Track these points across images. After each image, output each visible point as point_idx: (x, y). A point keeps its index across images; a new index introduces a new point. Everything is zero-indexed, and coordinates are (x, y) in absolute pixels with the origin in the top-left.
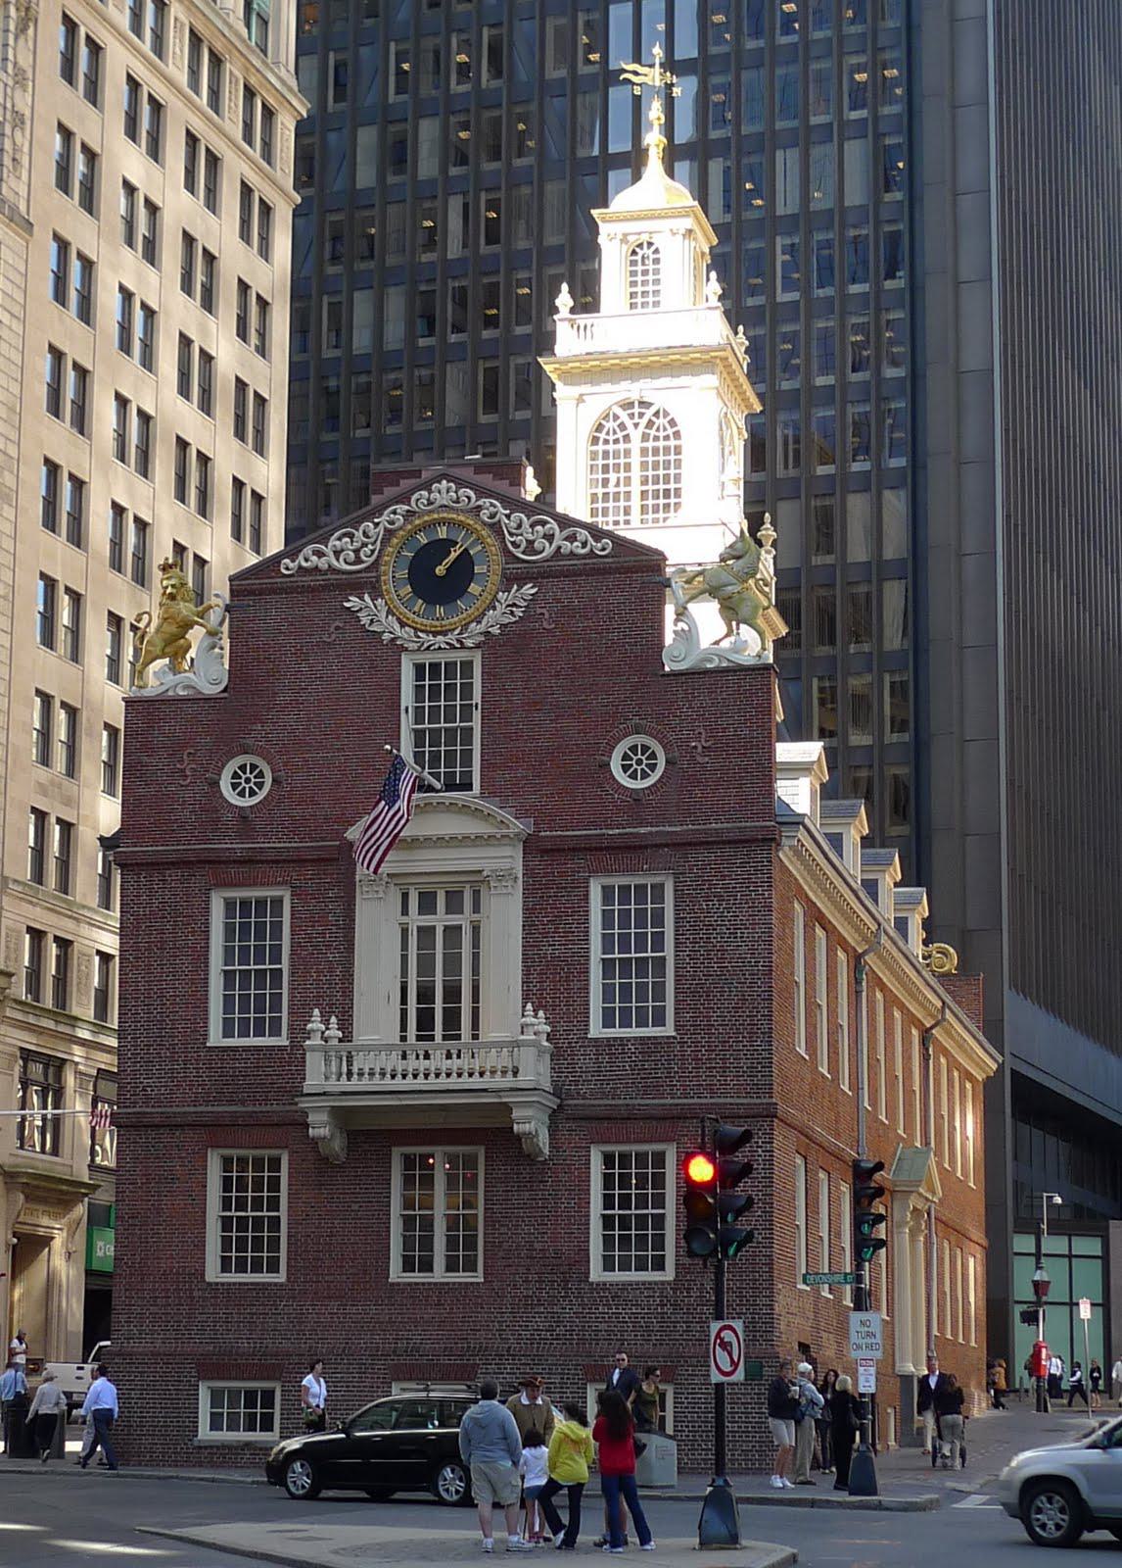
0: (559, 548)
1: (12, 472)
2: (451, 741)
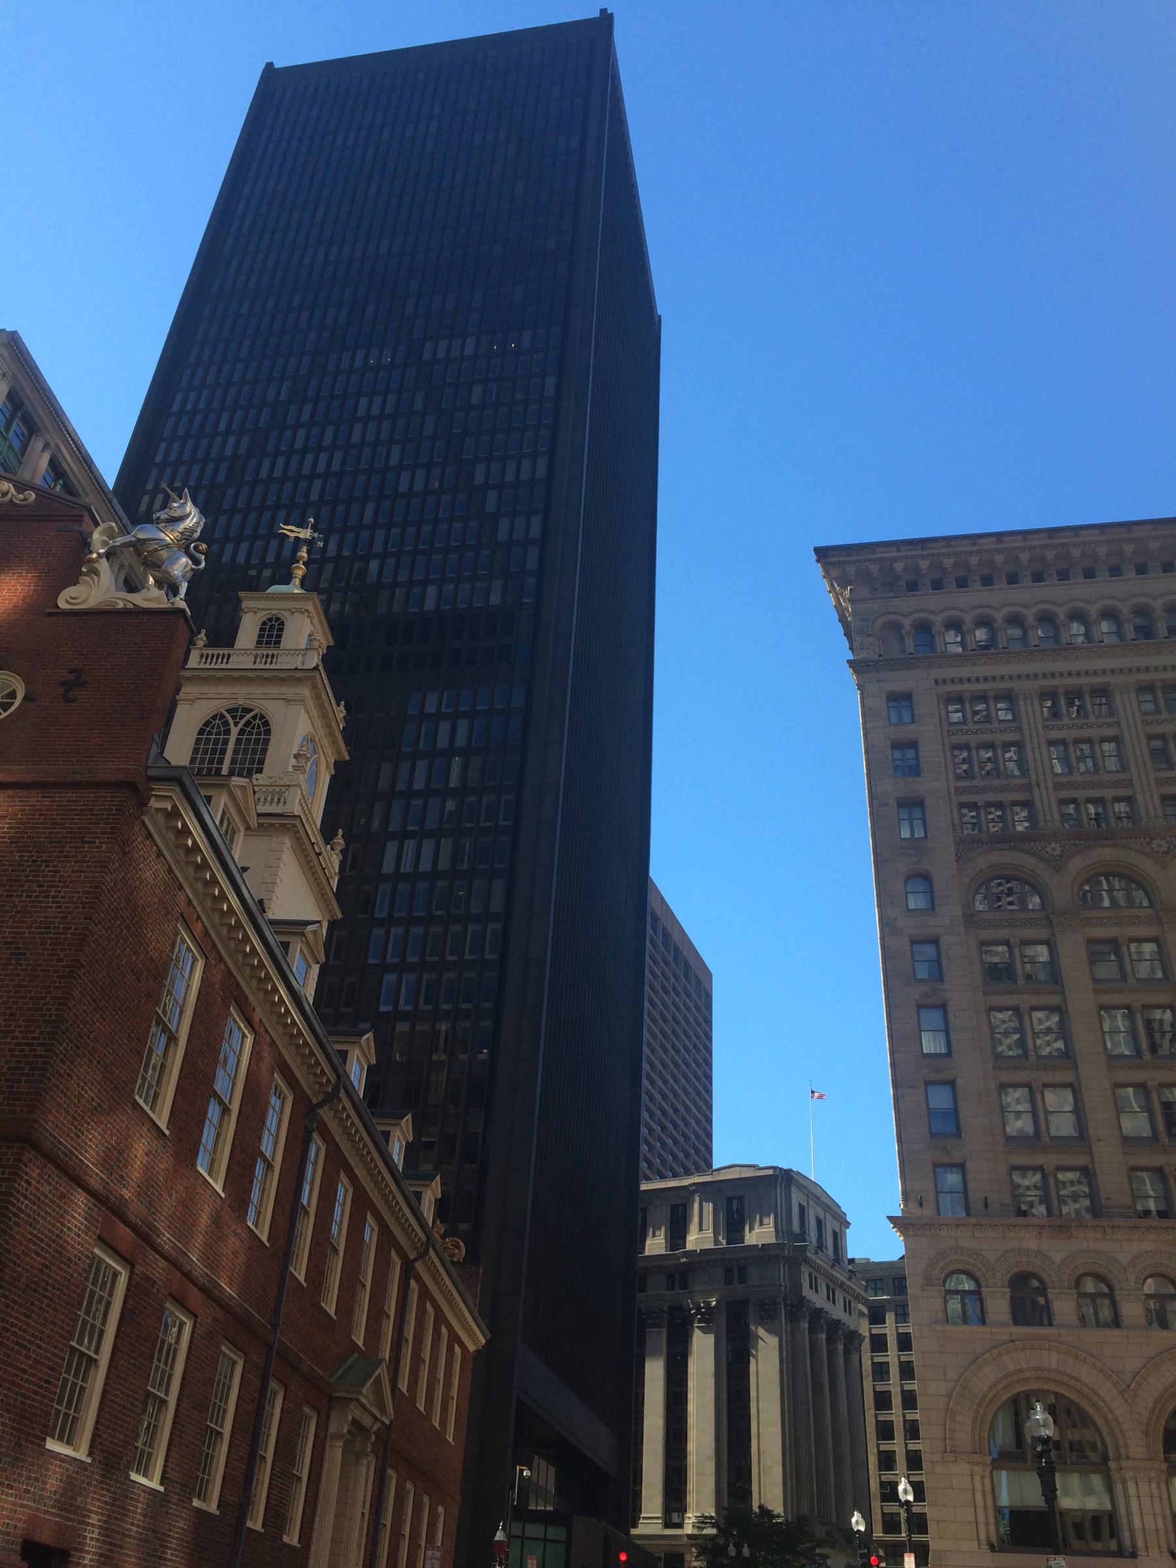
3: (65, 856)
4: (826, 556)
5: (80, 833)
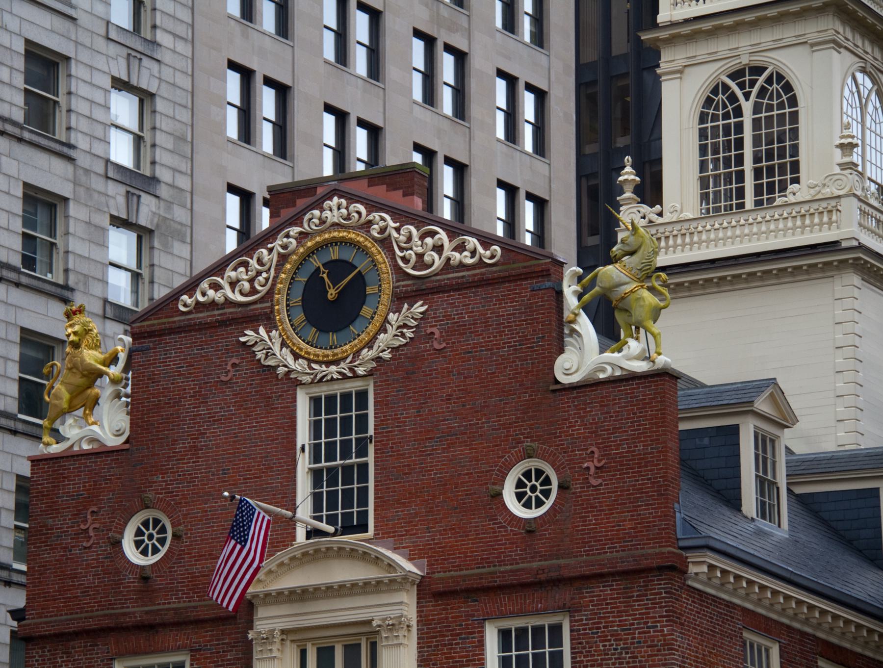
0: (449, 259)
1: (184, 206)
2: (347, 480)
3: (638, 642)
5: (642, 618)
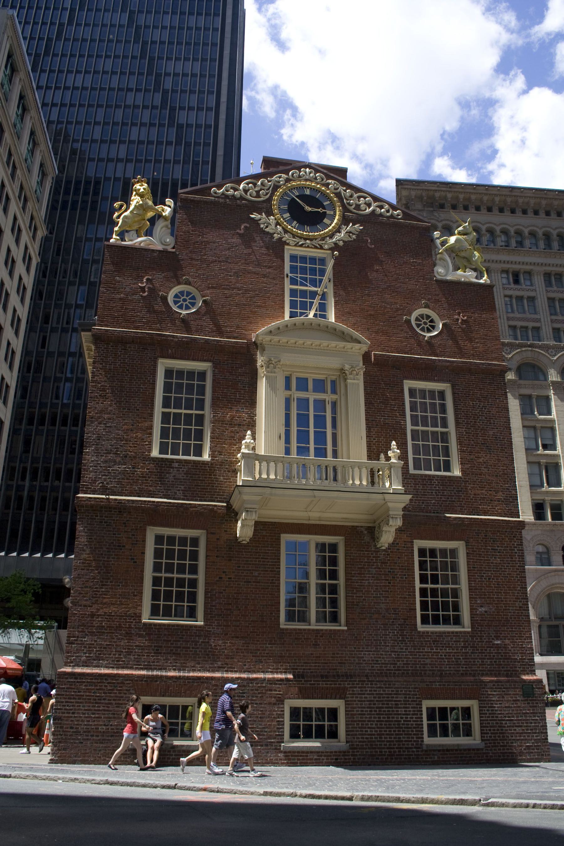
4: (402, 184)
